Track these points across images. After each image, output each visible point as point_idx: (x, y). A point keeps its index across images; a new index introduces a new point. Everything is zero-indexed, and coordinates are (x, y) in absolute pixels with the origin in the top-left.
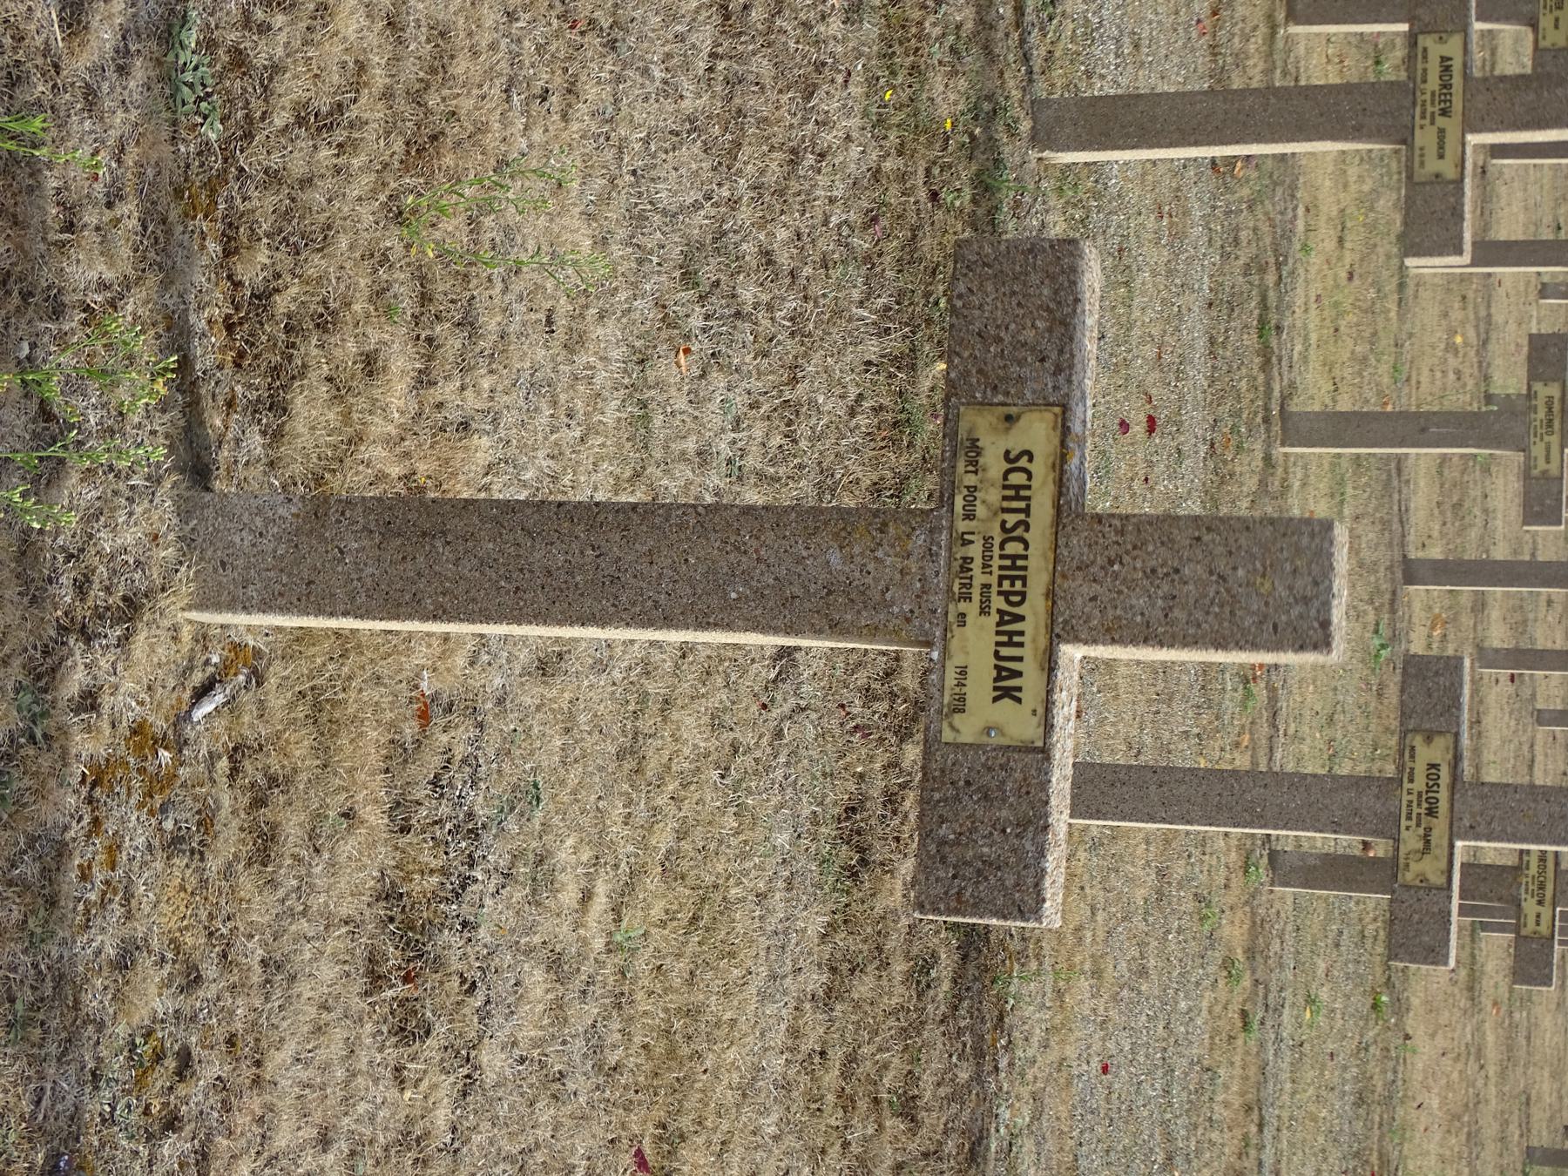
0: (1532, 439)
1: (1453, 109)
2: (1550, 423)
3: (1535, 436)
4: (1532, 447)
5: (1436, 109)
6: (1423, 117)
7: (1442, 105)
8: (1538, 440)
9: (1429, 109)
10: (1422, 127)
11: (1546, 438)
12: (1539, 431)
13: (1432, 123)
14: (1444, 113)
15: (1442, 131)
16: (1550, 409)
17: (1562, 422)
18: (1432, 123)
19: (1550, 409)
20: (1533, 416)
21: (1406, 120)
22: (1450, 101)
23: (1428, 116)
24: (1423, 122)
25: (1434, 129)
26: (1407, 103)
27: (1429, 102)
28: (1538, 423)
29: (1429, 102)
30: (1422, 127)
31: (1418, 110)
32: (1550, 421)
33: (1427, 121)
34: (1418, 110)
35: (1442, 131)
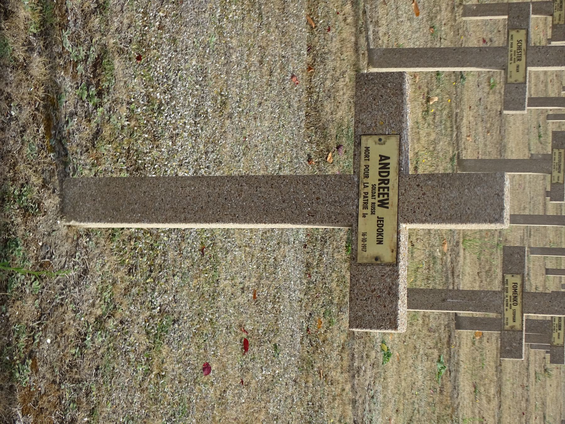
0: (505, 308)
1: (390, 201)
3: (507, 306)
4: (505, 312)
5: (376, 201)
6: (365, 207)
7: (381, 198)
8: (508, 308)
9: (371, 201)
10: (364, 216)
11: (513, 307)
13: (373, 213)
14: (383, 204)
15: (380, 220)
17: (522, 298)
18: (373, 213)
21: (352, 209)
22: (388, 194)
23: (369, 205)
24: (365, 211)
25: (374, 218)
26: (352, 195)
27: (370, 195)
29: (370, 195)
30: (364, 216)
31: (361, 200)
33: (369, 211)
34: (361, 200)
35: (380, 220)
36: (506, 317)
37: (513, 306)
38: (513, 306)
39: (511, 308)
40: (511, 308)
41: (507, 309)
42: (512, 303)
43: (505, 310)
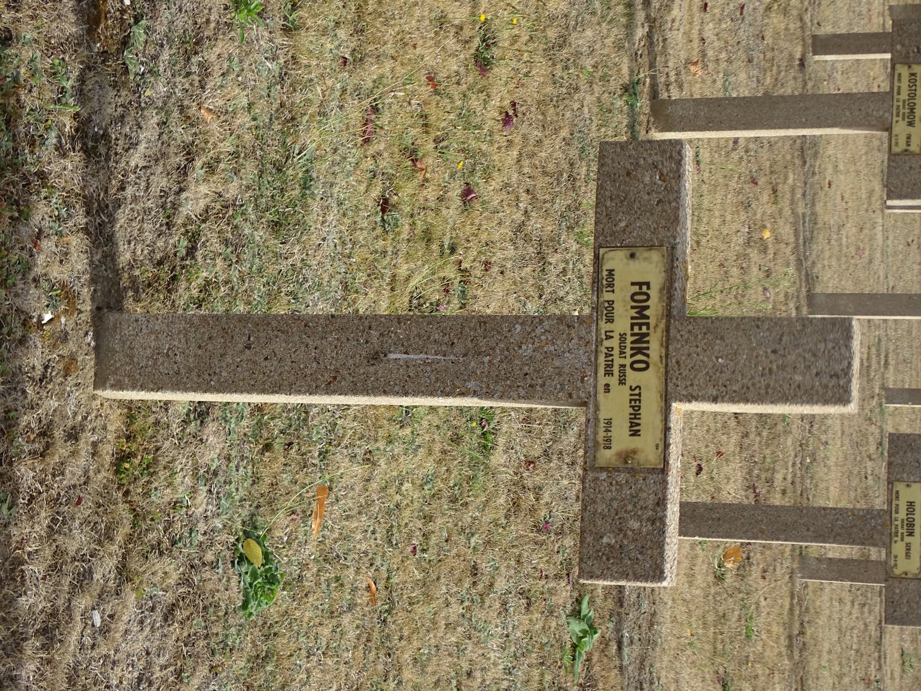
0: (602, 380)
2: (640, 344)
3: (608, 373)
4: (601, 396)
8: (613, 381)
11: (633, 378)
12: (618, 361)
16: (641, 311)
17: (667, 343)
19: (641, 311)
20: (604, 326)
28: (615, 343)
32: (641, 338)
36: (602, 415)
37: (631, 375)
38: (631, 375)
39: (622, 382)
40: (622, 382)
41: (607, 385)
42: (628, 361)
43: (601, 389)
